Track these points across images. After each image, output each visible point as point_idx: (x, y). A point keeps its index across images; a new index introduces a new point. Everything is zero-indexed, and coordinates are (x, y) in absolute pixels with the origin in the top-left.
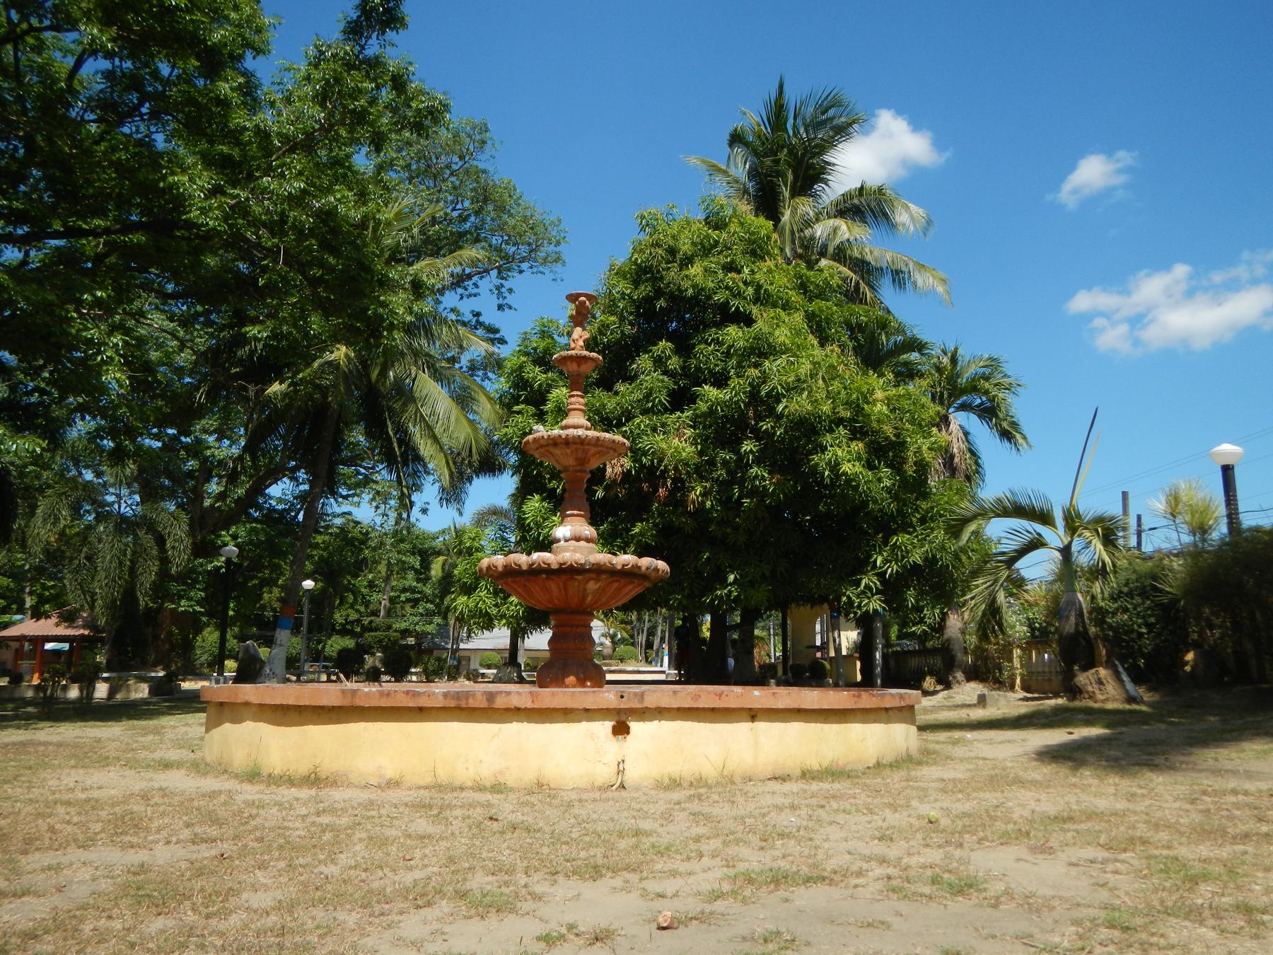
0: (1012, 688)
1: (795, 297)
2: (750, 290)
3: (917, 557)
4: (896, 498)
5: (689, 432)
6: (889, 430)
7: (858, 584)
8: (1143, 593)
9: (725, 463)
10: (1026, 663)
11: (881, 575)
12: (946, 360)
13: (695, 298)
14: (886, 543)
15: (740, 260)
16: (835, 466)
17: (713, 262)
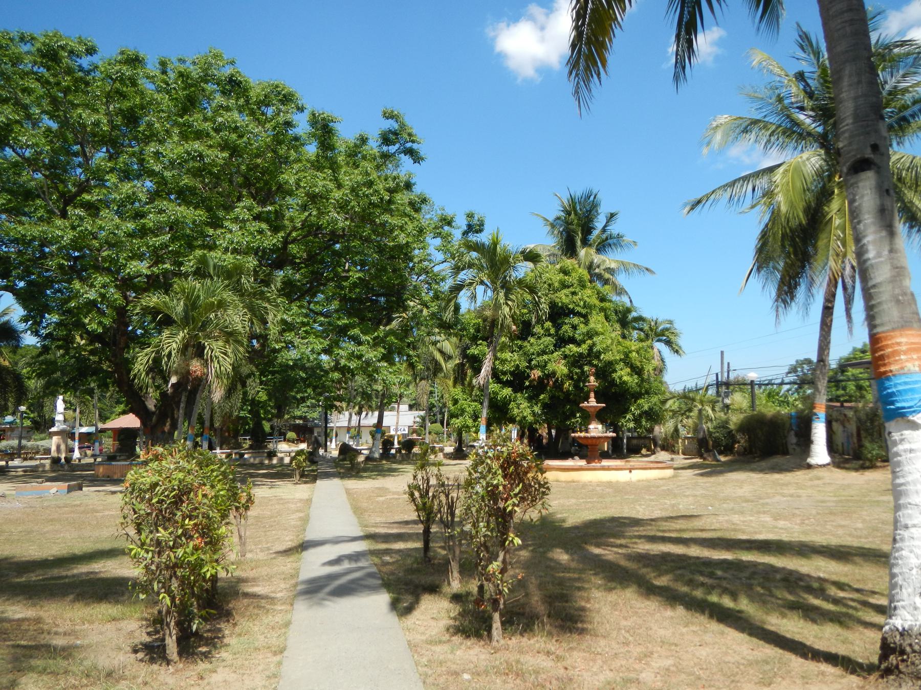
0: (678, 453)
1: (597, 302)
2: (582, 303)
3: (646, 408)
4: (639, 386)
5: (563, 361)
6: (639, 364)
7: (625, 417)
8: (723, 427)
9: (577, 373)
10: (684, 444)
11: (633, 415)
12: (653, 324)
13: (562, 307)
14: (635, 402)
15: (577, 290)
16: (620, 378)
17: (566, 291)
